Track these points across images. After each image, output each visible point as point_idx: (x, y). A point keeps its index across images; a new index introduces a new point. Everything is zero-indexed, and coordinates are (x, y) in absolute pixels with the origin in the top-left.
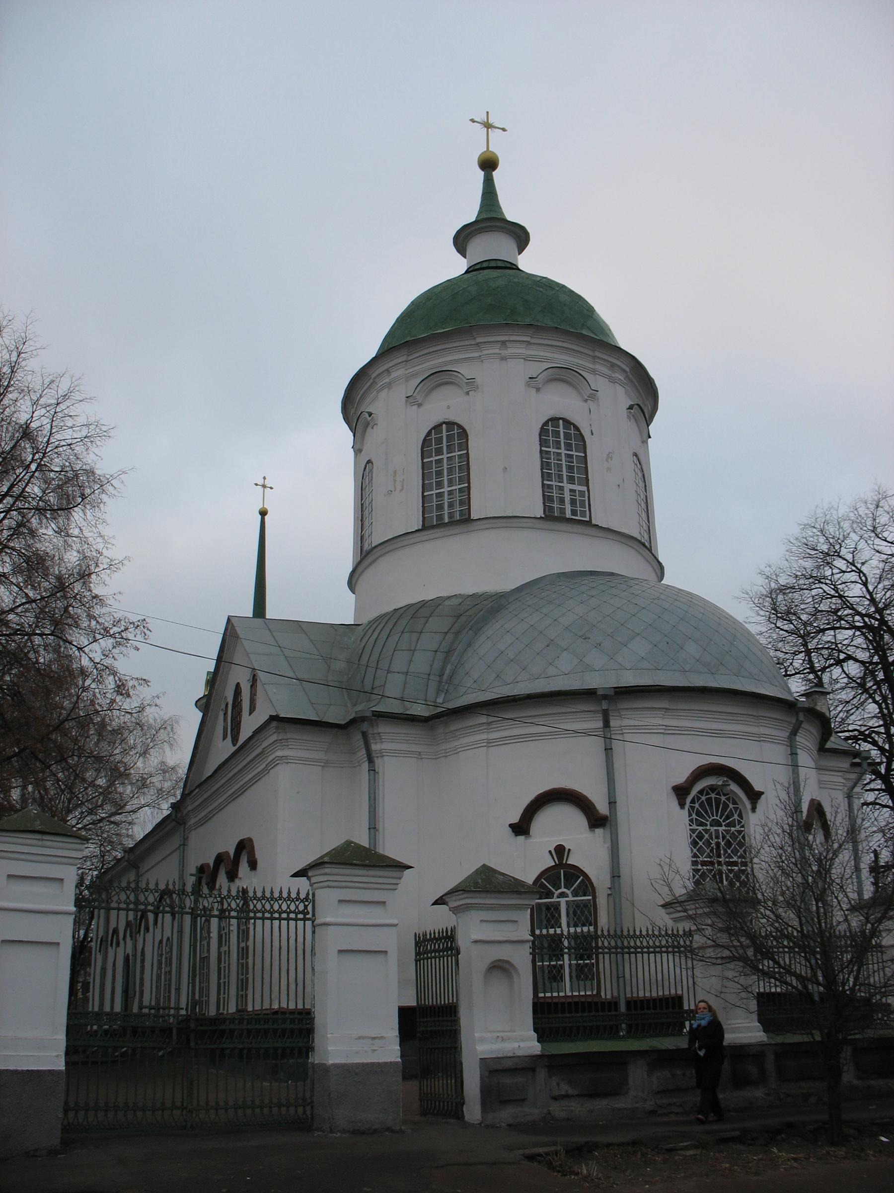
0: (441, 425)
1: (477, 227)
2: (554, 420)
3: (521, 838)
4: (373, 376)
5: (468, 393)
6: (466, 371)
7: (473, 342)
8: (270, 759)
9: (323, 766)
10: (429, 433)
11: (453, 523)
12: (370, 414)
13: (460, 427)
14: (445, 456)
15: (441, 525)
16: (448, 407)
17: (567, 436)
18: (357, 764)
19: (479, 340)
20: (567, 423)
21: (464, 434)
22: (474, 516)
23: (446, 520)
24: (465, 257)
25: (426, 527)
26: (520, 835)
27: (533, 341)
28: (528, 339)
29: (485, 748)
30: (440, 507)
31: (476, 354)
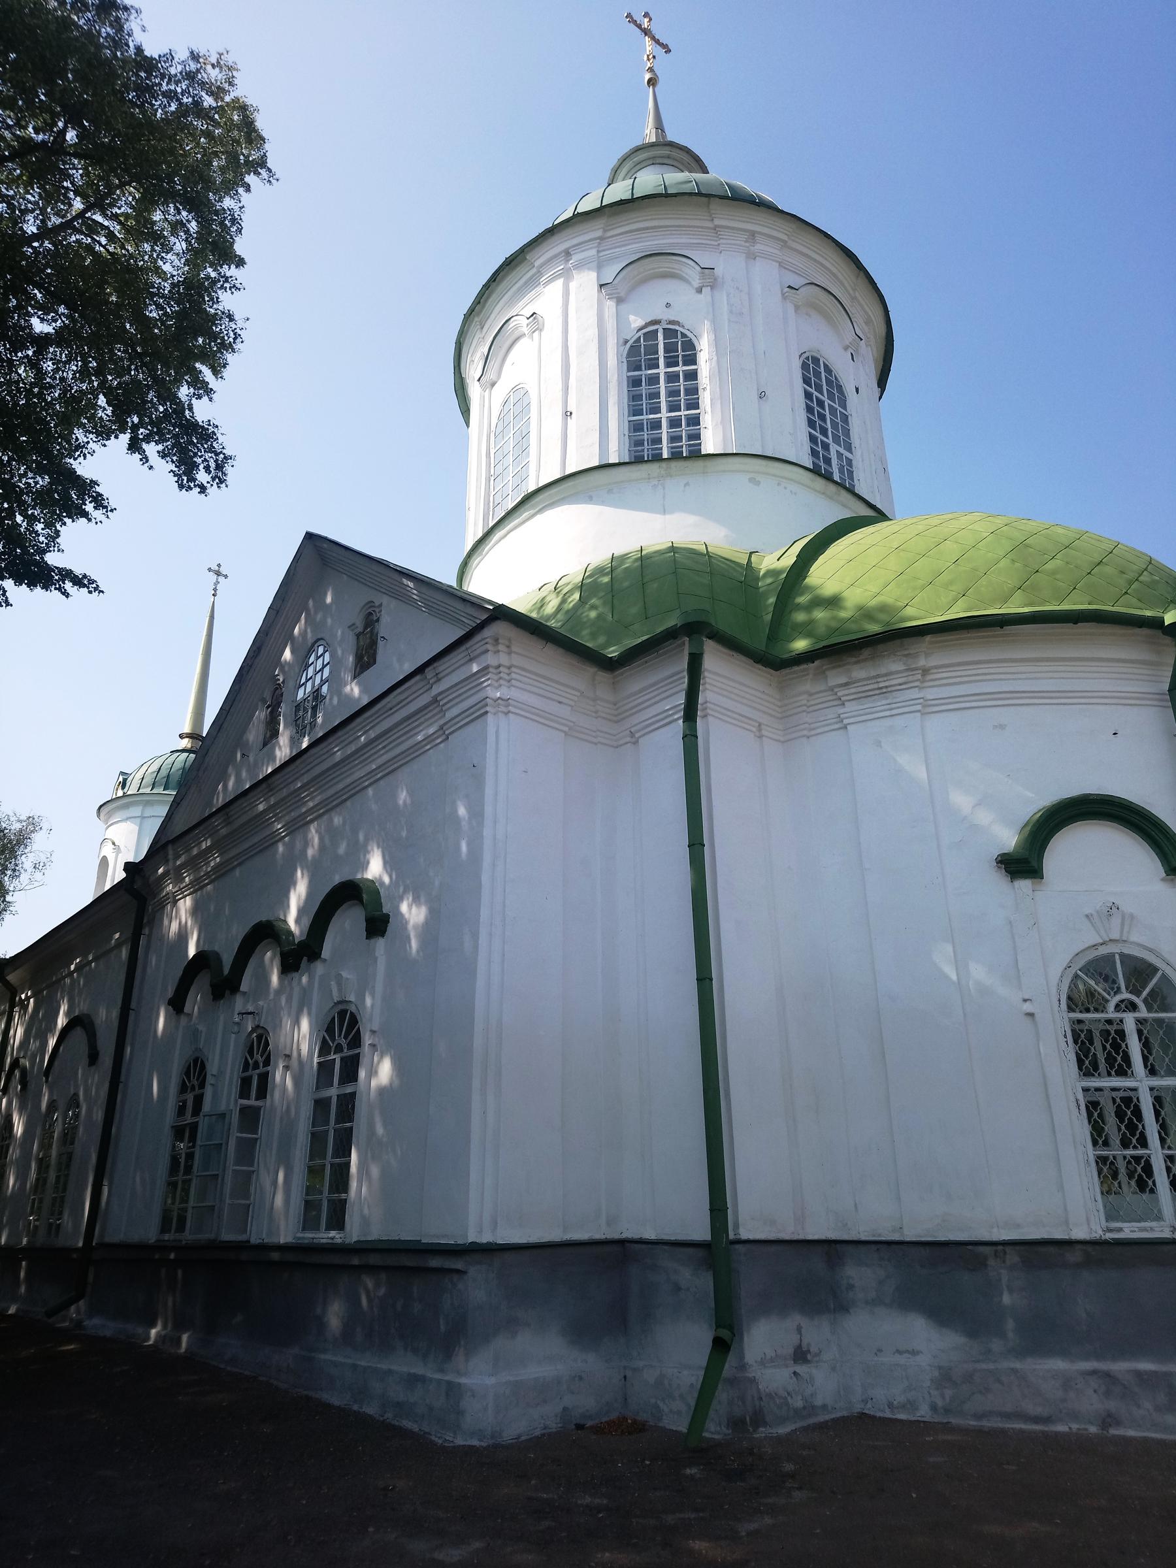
3: (1024, 885)
4: (537, 264)
5: (699, 291)
8: (449, 715)
9: (566, 734)
16: (668, 305)
17: (829, 382)
18: (628, 739)
20: (828, 370)
26: (1026, 878)
27: (790, 243)
28: (785, 238)
29: (918, 714)
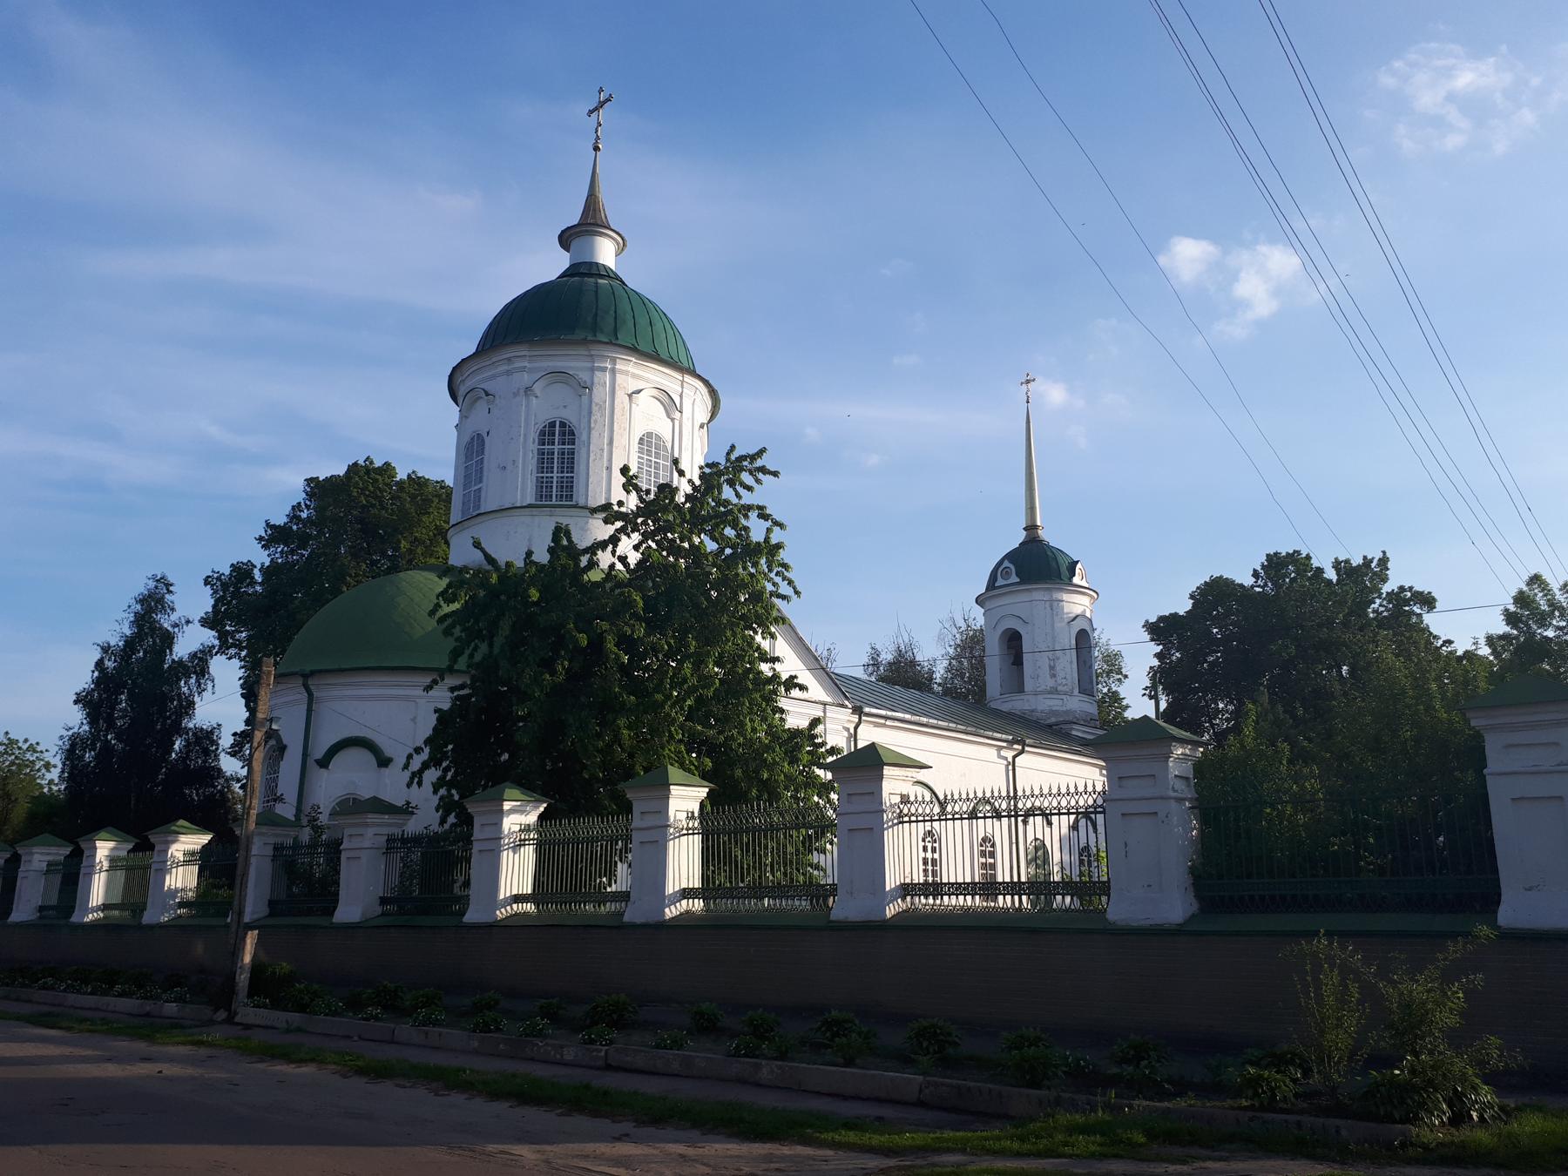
1: (578, 230)
2: (649, 435)
7: (586, 353)
12: (487, 394)
14: (556, 447)
19: (593, 353)
20: (658, 437)
31: (589, 365)
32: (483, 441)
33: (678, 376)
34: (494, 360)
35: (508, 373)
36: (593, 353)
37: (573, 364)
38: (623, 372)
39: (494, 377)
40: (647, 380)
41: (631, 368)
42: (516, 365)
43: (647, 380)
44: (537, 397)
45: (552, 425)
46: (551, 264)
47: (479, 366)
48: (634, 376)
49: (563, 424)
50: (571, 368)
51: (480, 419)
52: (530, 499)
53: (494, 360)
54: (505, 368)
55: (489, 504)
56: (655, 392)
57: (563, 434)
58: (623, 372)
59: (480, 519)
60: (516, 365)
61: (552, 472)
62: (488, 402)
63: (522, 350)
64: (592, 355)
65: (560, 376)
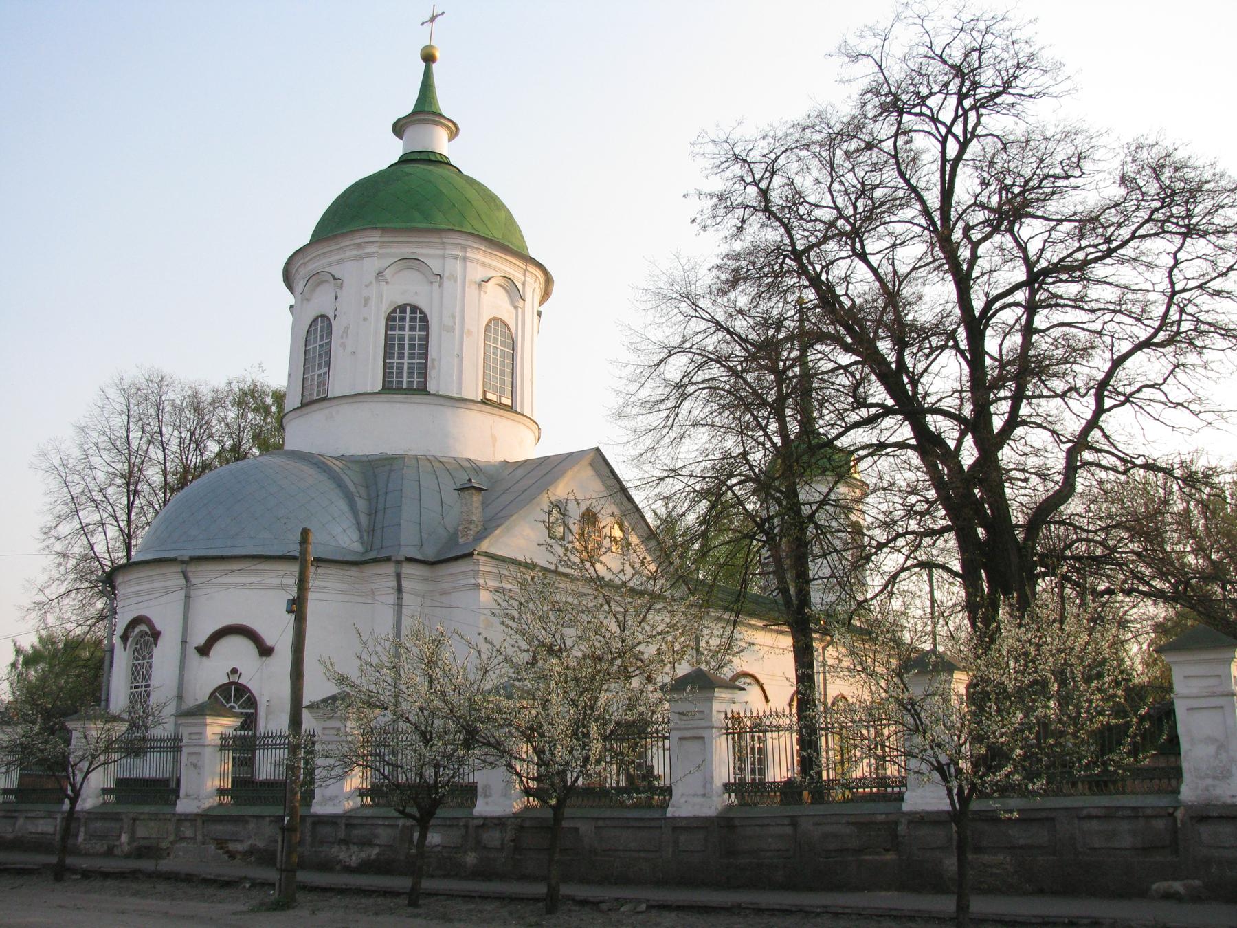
0: (405, 305)
6: (435, 265)
10: (394, 311)
11: (410, 391)
12: (335, 278)
13: (421, 312)
14: (407, 333)
15: (399, 390)
19: (445, 240)
21: (424, 319)
22: (432, 387)
23: (405, 387)
24: (402, 138)
25: (388, 388)
30: (400, 375)
31: (440, 252)
32: (330, 325)
33: (521, 264)
34: (343, 244)
35: (359, 258)
36: (445, 240)
37: (424, 251)
38: (472, 260)
39: (342, 261)
40: (495, 269)
41: (480, 256)
42: (367, 251)
43: (495, 269)
44: (387, 283)
45: (402, 308)
46: (390, 151)
47: (319, 252)
48: (483, 264)
49: (414, 309)
50: (422, 255)
51: (322, 302)
52: (380, 387)
53: (342, 245)
54: (354, 253)
55: (336, 389)
56: (502, 281)
57: (412, 319)
58: (472, 260)
59: (325, 404)
60: (367, 251)
61: (403, 358)
62: (336, 287)
63: (373, 236)
64: (443, 243)
65: (412, 262)
